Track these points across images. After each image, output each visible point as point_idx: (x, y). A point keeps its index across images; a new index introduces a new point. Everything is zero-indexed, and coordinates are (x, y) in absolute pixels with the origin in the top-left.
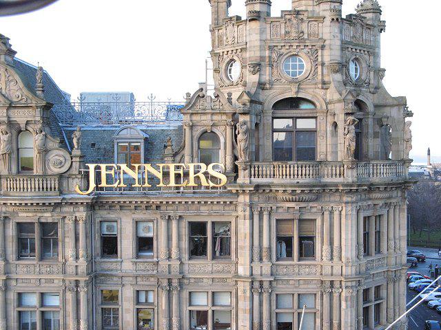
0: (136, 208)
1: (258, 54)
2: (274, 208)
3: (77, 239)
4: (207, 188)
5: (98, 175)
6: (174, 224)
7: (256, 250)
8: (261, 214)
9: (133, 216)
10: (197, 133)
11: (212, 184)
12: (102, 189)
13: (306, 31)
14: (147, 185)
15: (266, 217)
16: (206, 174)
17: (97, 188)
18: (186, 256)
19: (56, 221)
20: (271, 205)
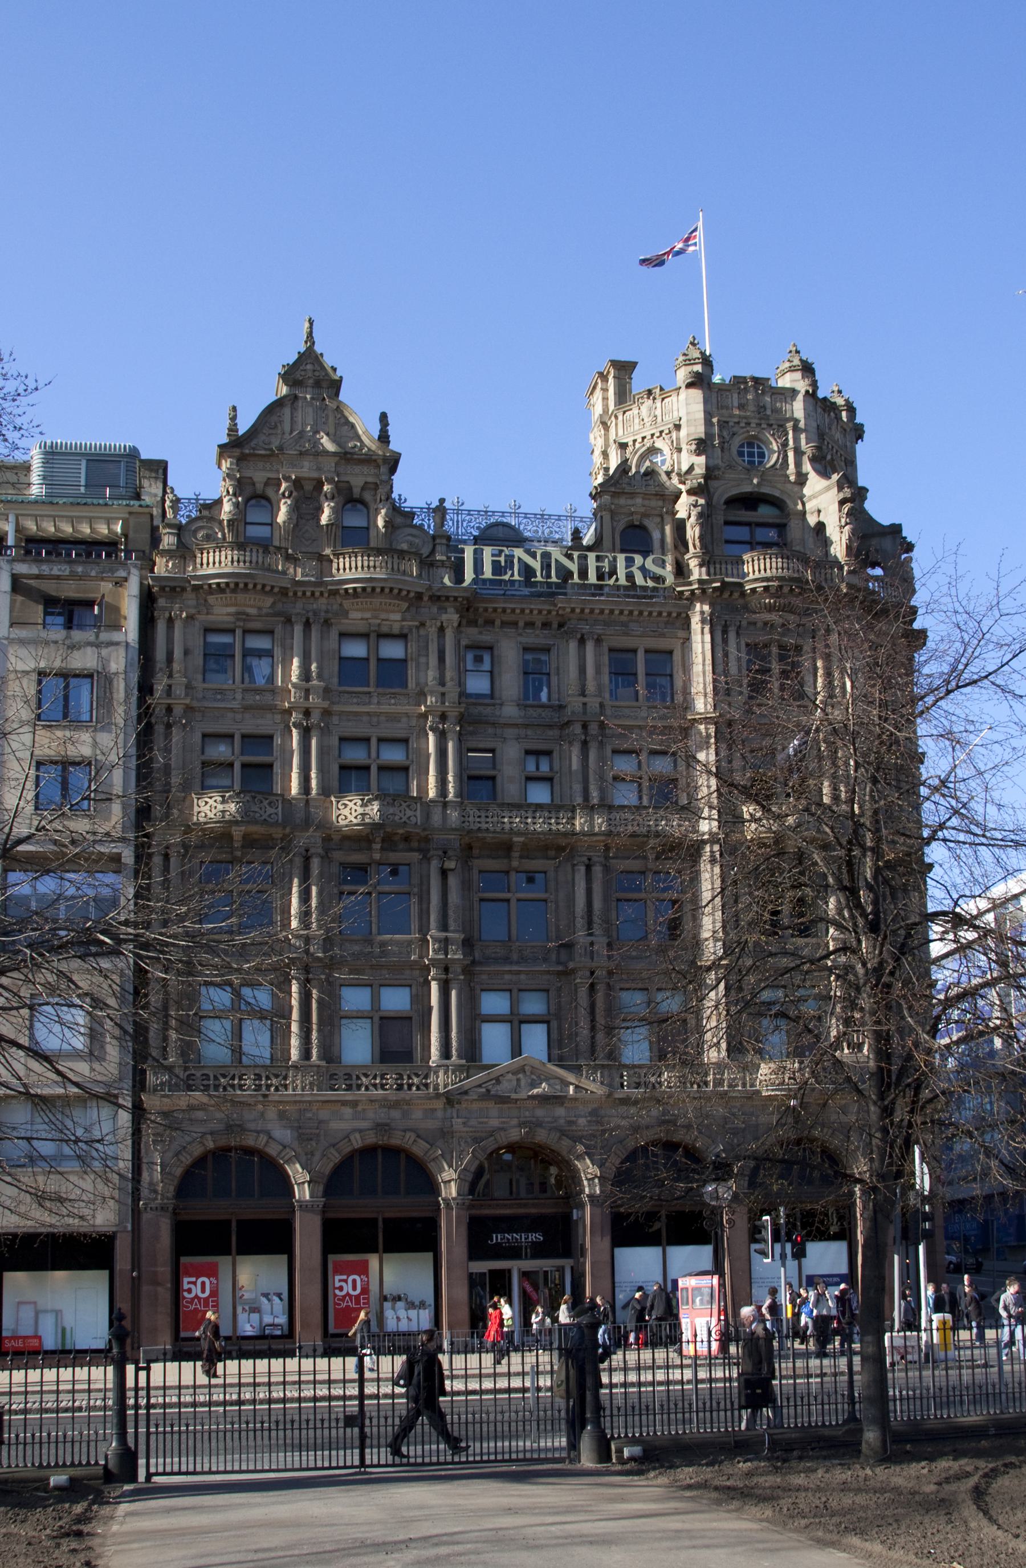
0: (530, 624)
2: (744, 623)
3: (442, 659)
4: (641, 587)
6: (590, 647)
8: (725, 631)
11: (650, 584)
13: (768, 406)
14: (554, 579)
15: (732, 635)
16: (642, 569)
17: (475, 581)
19: (405, 631)
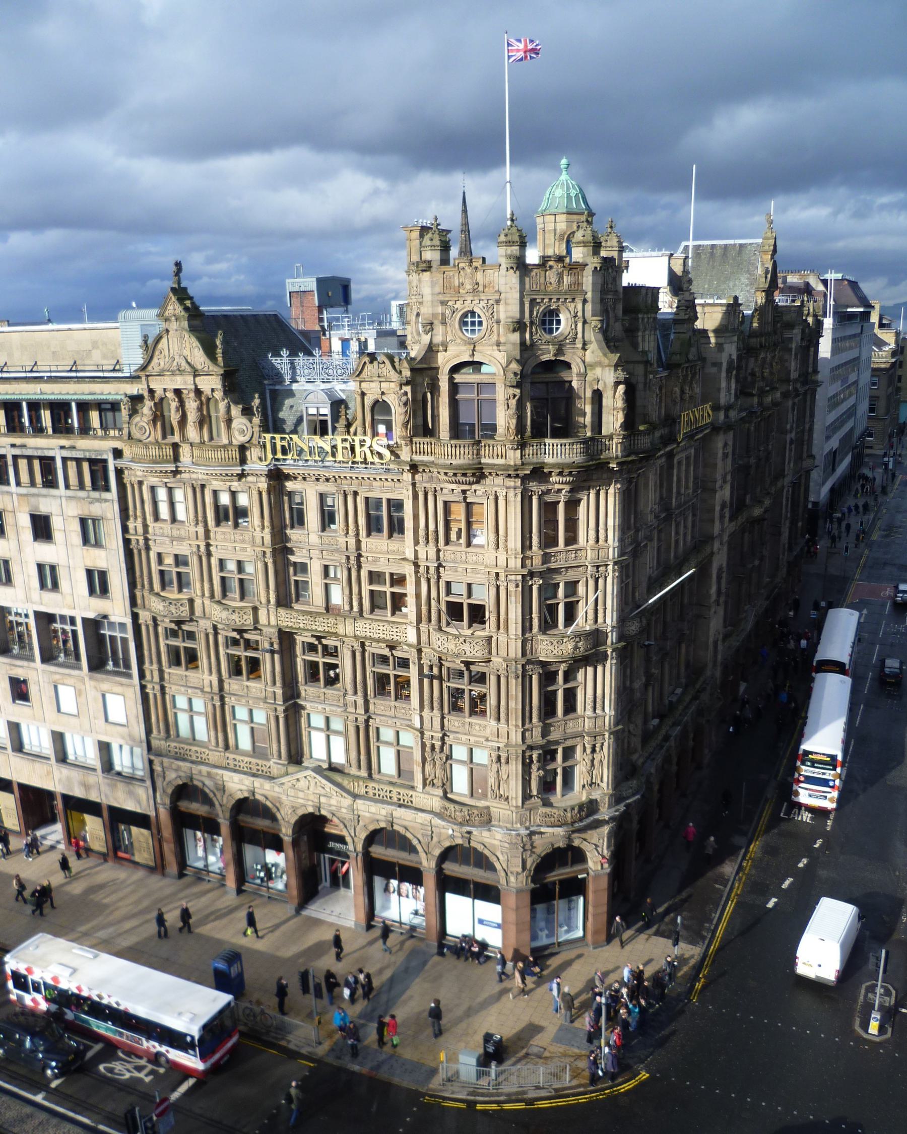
1: (430, 311)
2: (438, 488)
5: (274, 446)
7: (422, 532)
9: (317, 488)
10: (368, 402)
12: (278, 460)
18: (363, 532)
20: (434, 486)
